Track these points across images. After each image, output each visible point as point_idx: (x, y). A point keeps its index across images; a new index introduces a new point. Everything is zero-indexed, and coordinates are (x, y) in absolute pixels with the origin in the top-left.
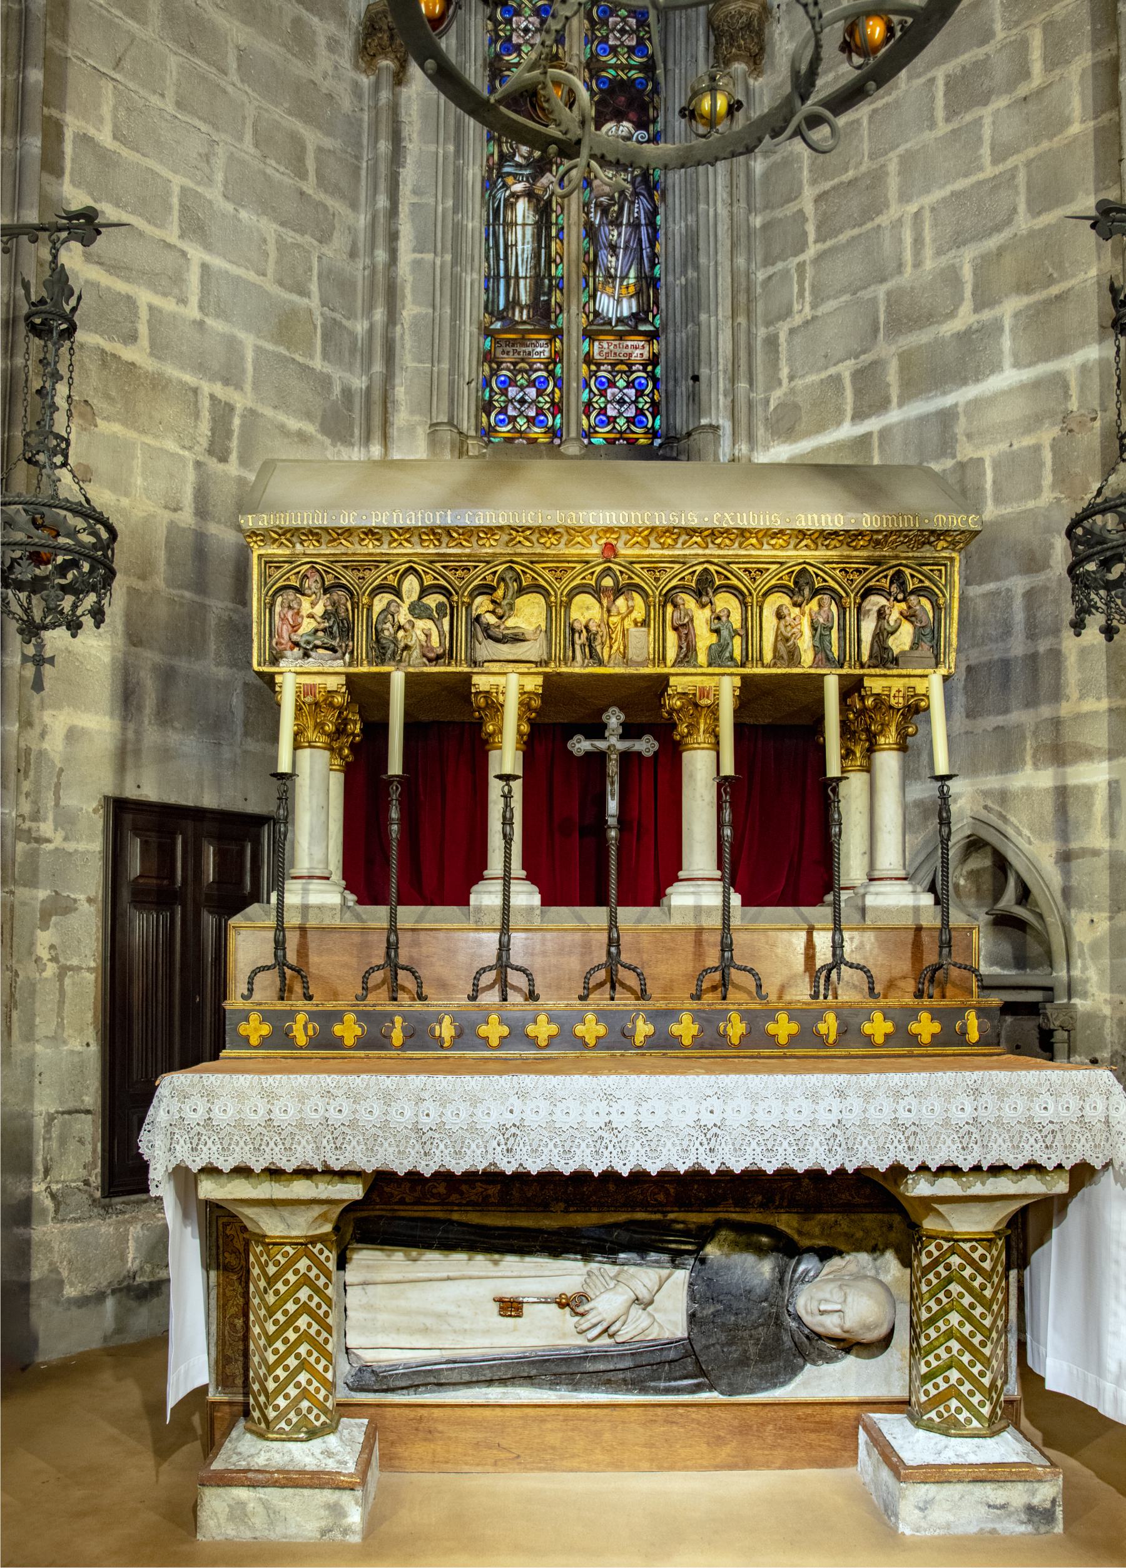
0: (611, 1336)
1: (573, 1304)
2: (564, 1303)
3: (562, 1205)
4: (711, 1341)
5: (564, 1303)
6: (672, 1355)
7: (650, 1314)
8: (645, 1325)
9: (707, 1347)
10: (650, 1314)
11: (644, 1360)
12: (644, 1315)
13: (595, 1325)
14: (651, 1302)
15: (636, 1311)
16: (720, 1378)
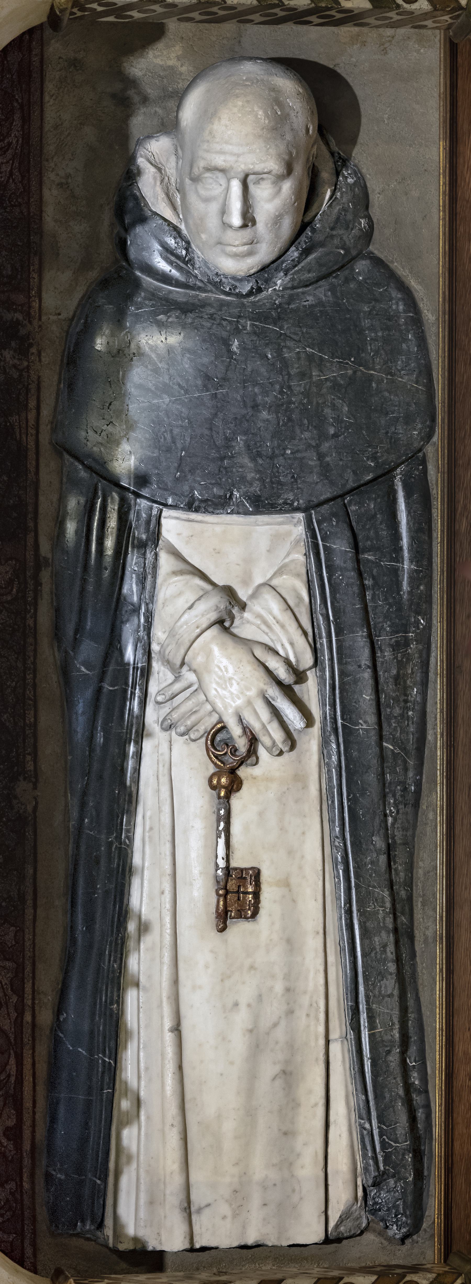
0: (300, 676)
1: (231, 761)
2: (227, 781)
3: (22, 786)
4: (313, 462)
5: (227, 781)
6: (341, 546)
7: (254, 596)
8: (275, 606)
9: (325, 470)
10: (254, 596)
11: (352, 607)
12: (255, 607)
13: (276, 713)
14: (229, 592)
15: (247, 626)
16: (394, 442)
